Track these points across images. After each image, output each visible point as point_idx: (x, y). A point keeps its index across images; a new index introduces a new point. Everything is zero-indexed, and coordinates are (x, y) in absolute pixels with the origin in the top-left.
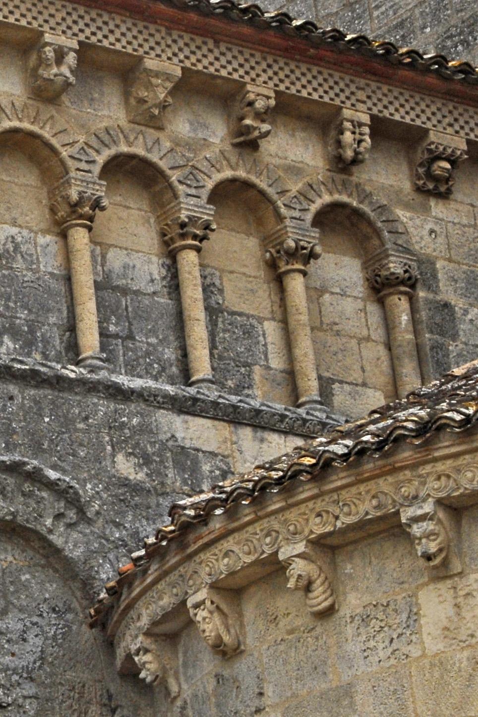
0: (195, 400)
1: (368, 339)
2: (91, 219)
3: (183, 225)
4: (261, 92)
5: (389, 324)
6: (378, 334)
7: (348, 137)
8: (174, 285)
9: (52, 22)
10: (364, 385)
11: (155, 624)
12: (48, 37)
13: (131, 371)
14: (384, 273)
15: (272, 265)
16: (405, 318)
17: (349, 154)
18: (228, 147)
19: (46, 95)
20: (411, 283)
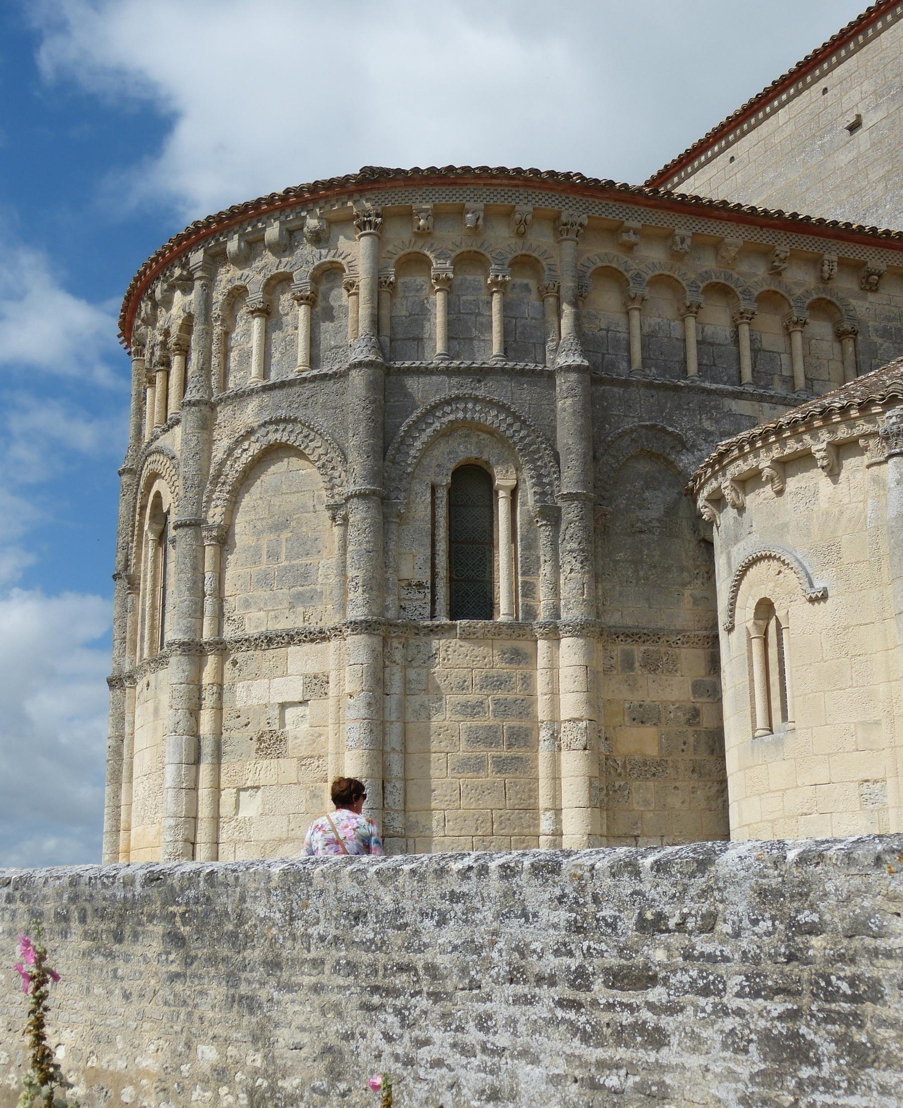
0: (742, 393)
1: (833, 359)
2: (696, 313)
3: (742, 313)
4: (783, 249)
5: (843, 352)
6: (838, 357)
7: (826, 268)
8: (736, 340)
9: (680, 225)
10: (829, 380)
11: (709, 495)
12: (677, 232)
13: (714, 380)
14: (841, 329)
15: (787, 328)
16: (851, 349)
17: (826, 276)
18: (766, 276)
19: (677, 256)
20: (855, 333)
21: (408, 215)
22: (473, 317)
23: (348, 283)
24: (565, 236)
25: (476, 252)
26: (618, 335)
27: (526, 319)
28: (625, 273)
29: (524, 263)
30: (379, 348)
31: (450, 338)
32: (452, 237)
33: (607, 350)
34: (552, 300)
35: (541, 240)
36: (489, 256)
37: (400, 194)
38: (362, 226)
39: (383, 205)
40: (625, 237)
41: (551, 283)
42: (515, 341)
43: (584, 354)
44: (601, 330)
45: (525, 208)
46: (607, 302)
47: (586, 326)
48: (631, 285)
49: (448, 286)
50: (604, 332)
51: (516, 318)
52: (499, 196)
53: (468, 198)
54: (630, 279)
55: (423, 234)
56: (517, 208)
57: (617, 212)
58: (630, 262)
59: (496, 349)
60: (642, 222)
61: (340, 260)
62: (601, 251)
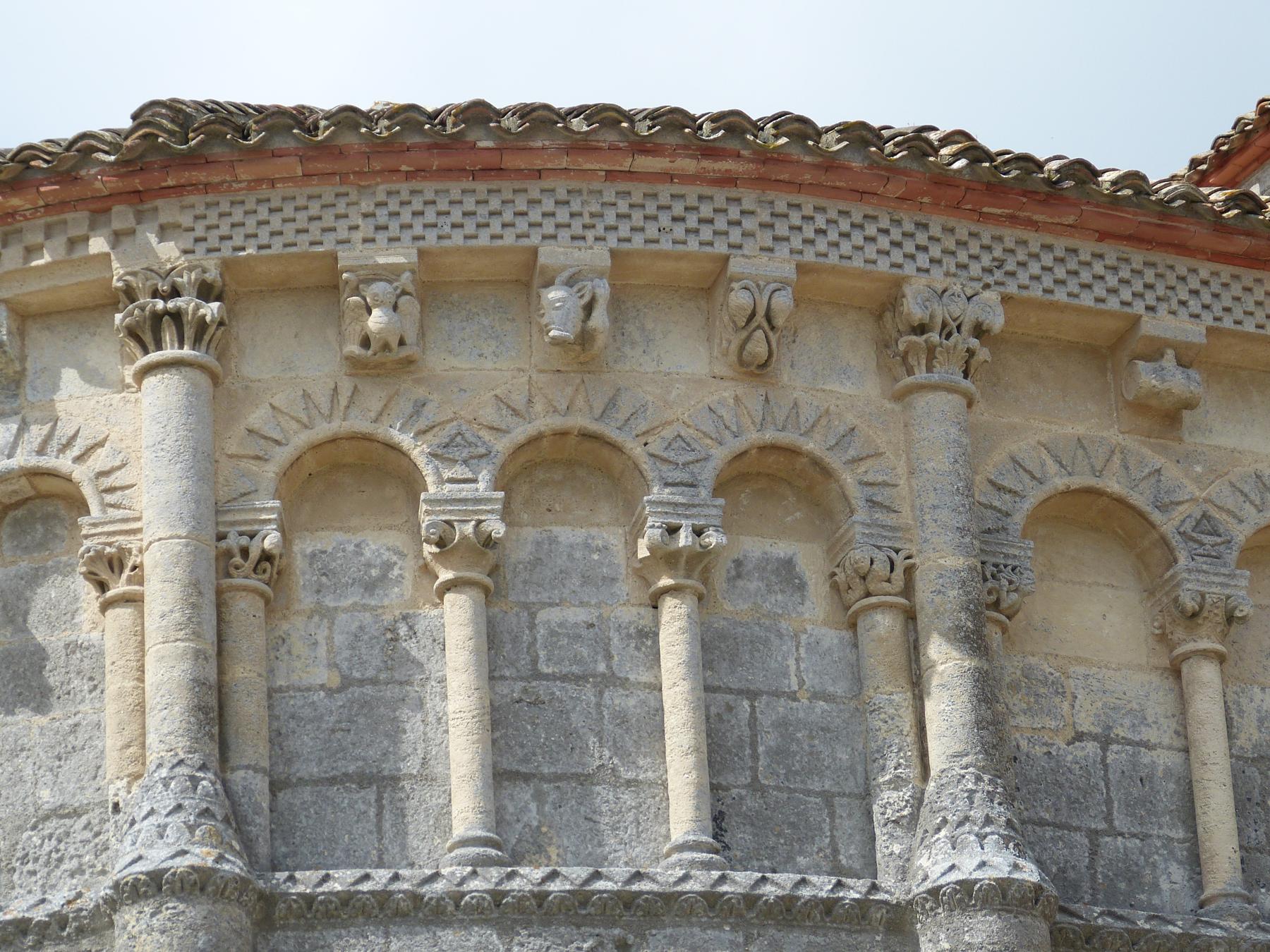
21: (325, 288)
22: (589, 693)
23: (99, 556)
24: (921, 376)
25: (586, 435)
26: (1146, 757)
27: (793, 697)
28: (1156, 517)
29: (774, 477)
30: (231, 817)
31: (500, 777)
32: (492, 379)
33: (1108, 818)
34: (885, 624)
35: (833, 387)
36: (637, 450)
37: (288, 211)
38: (146, 333)
39: (226, 251)
40: (1147, 377)
41: (880, 557)
42: (755, 786)
43: (1021, 835)
44: (1079, 737)
45: (763, 266)
46: (1094, 626)
47: (1024, 728)
48: (1183, 560)
49: (486, 568)
50: (1091, 748)
51: (752, 695)
52: (664, 219)
53: (549, 228)
54: (1175, 541)
55: (382, 364)
56: (735, 266)
57: (1112, 281)
58: (1172, 472)
59: (683, 816)
60: (1208, 319)
61: (64, 463)
62: (1058, 433)
